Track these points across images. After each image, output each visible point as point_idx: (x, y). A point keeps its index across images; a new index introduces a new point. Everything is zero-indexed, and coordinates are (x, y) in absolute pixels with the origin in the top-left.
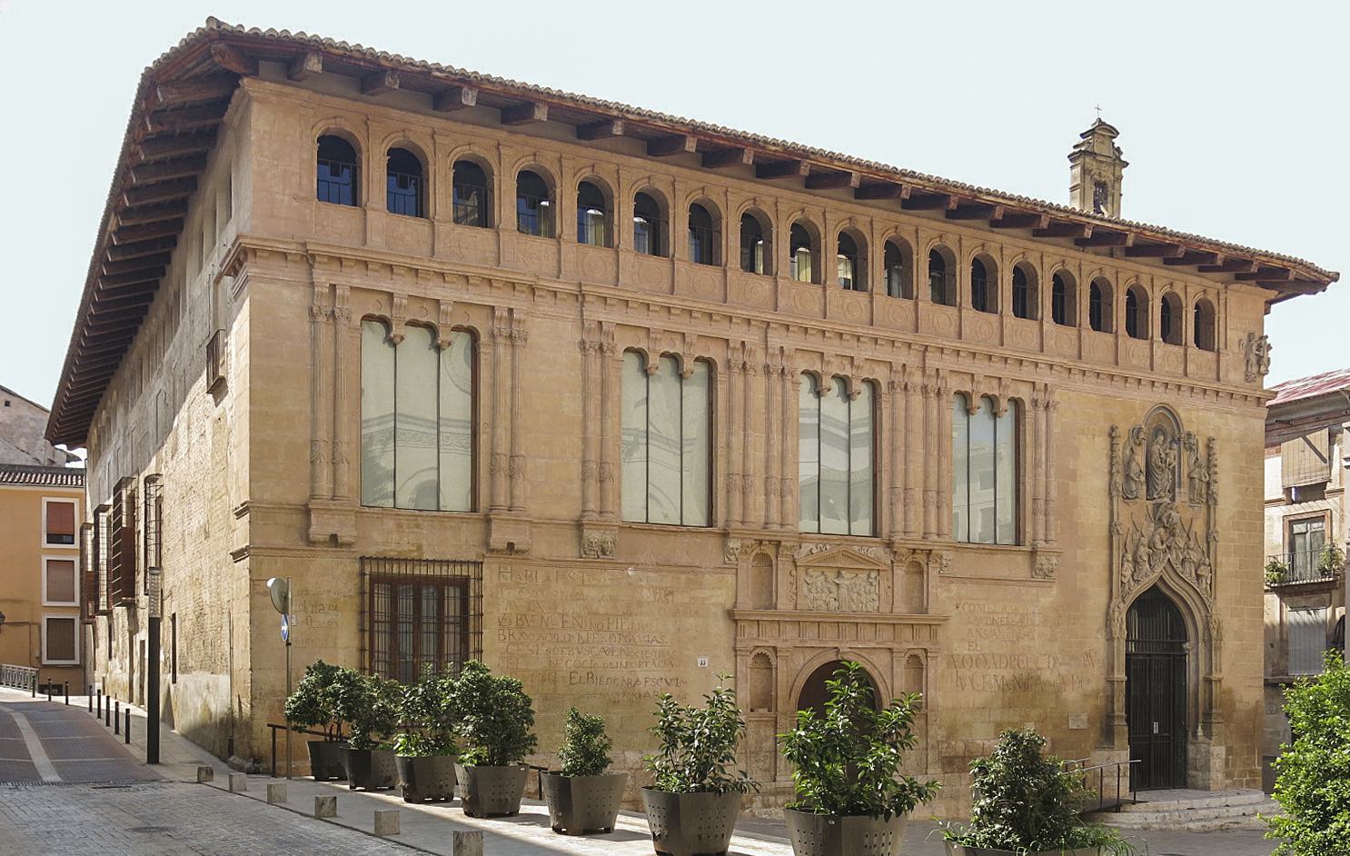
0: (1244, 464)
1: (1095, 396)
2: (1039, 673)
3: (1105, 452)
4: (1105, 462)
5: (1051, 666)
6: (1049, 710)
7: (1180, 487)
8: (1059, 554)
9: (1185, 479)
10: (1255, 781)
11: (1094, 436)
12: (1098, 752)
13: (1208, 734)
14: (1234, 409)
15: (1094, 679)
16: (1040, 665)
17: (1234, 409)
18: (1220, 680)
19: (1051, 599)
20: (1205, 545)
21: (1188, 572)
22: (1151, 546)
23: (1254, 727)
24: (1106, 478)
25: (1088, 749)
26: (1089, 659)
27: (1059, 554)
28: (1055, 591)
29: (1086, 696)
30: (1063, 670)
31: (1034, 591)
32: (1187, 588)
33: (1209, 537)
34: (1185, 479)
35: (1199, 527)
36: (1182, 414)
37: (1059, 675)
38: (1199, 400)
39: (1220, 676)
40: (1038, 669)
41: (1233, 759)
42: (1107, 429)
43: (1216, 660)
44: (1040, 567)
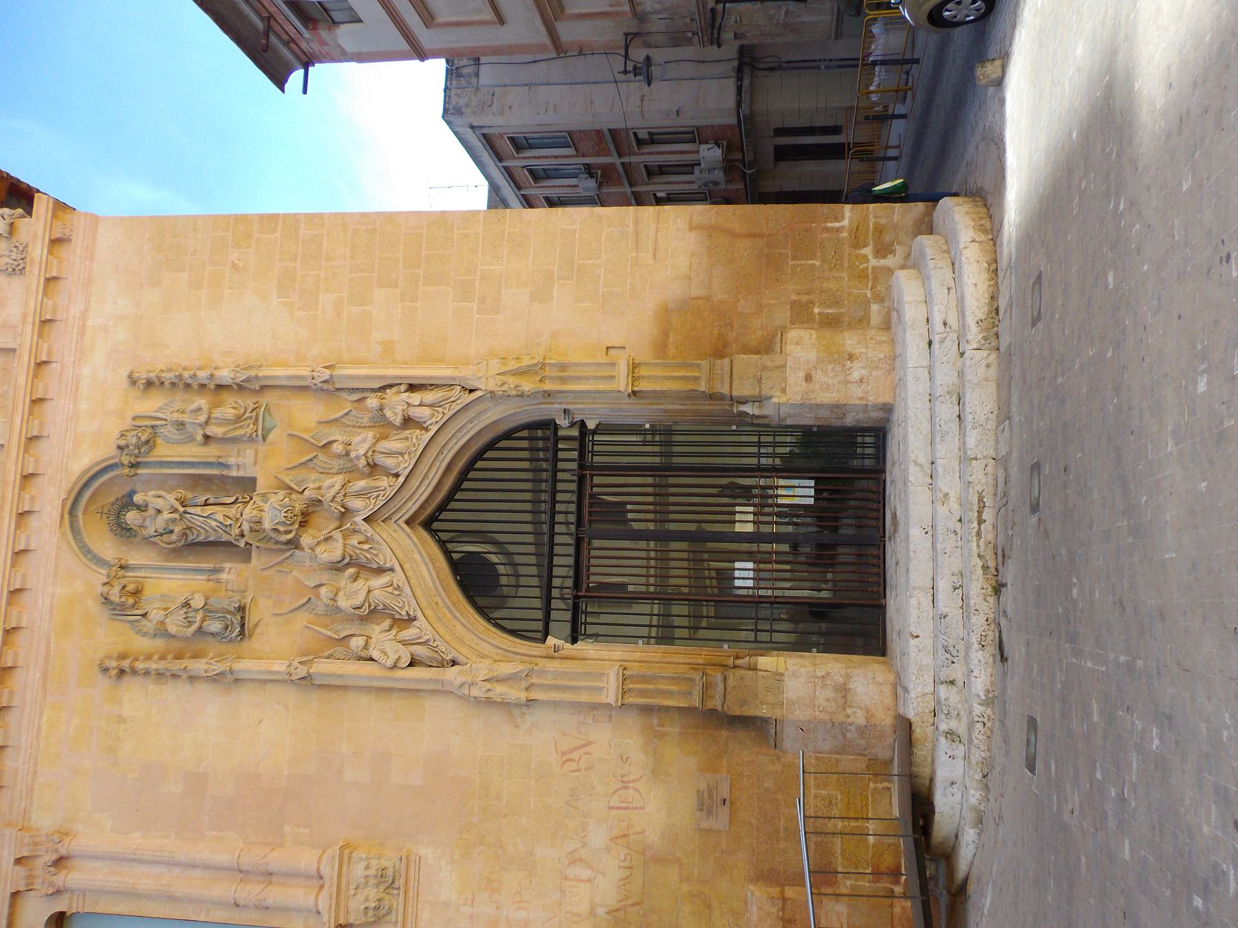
0: (185, 276)
1: (46, 712)
2: (601, 912)
3: (151, 687)
4: (171, 693)
5: (586, 873)
6: (686, 888)
7: (227, 466)
8: (346, 852)
9: (212, 452)
10: (879, 230)
11: (121, 720)
12: (787, 744)
13: (759, 400)
14: (75, 311)
15: (617, 746)
16: (583, 908)
17: (75, 311)
18: (634, 366)
19: (443, 863)
20: (344, 395)
21: (399, 451)
22: (337, 567)
23: (751, 236)
24: (202, 687)
25: (778, 767)
26: (575, 755)
27: (346, 852)
28: (427, 852)
29: (657, 771)
30: (598, 837)
31: (425, 914)
32: (433, 451)
33: (329, 389)
34: (212, 452)
35: (306, 414)
36: (83, 461)
37: (608, 850)
38: (56, 415)
39: (622, 368)
40: (592, 912)
41: (823, 304)
42: (103, 682)
43: (587, 378)
44: (371, 913)
